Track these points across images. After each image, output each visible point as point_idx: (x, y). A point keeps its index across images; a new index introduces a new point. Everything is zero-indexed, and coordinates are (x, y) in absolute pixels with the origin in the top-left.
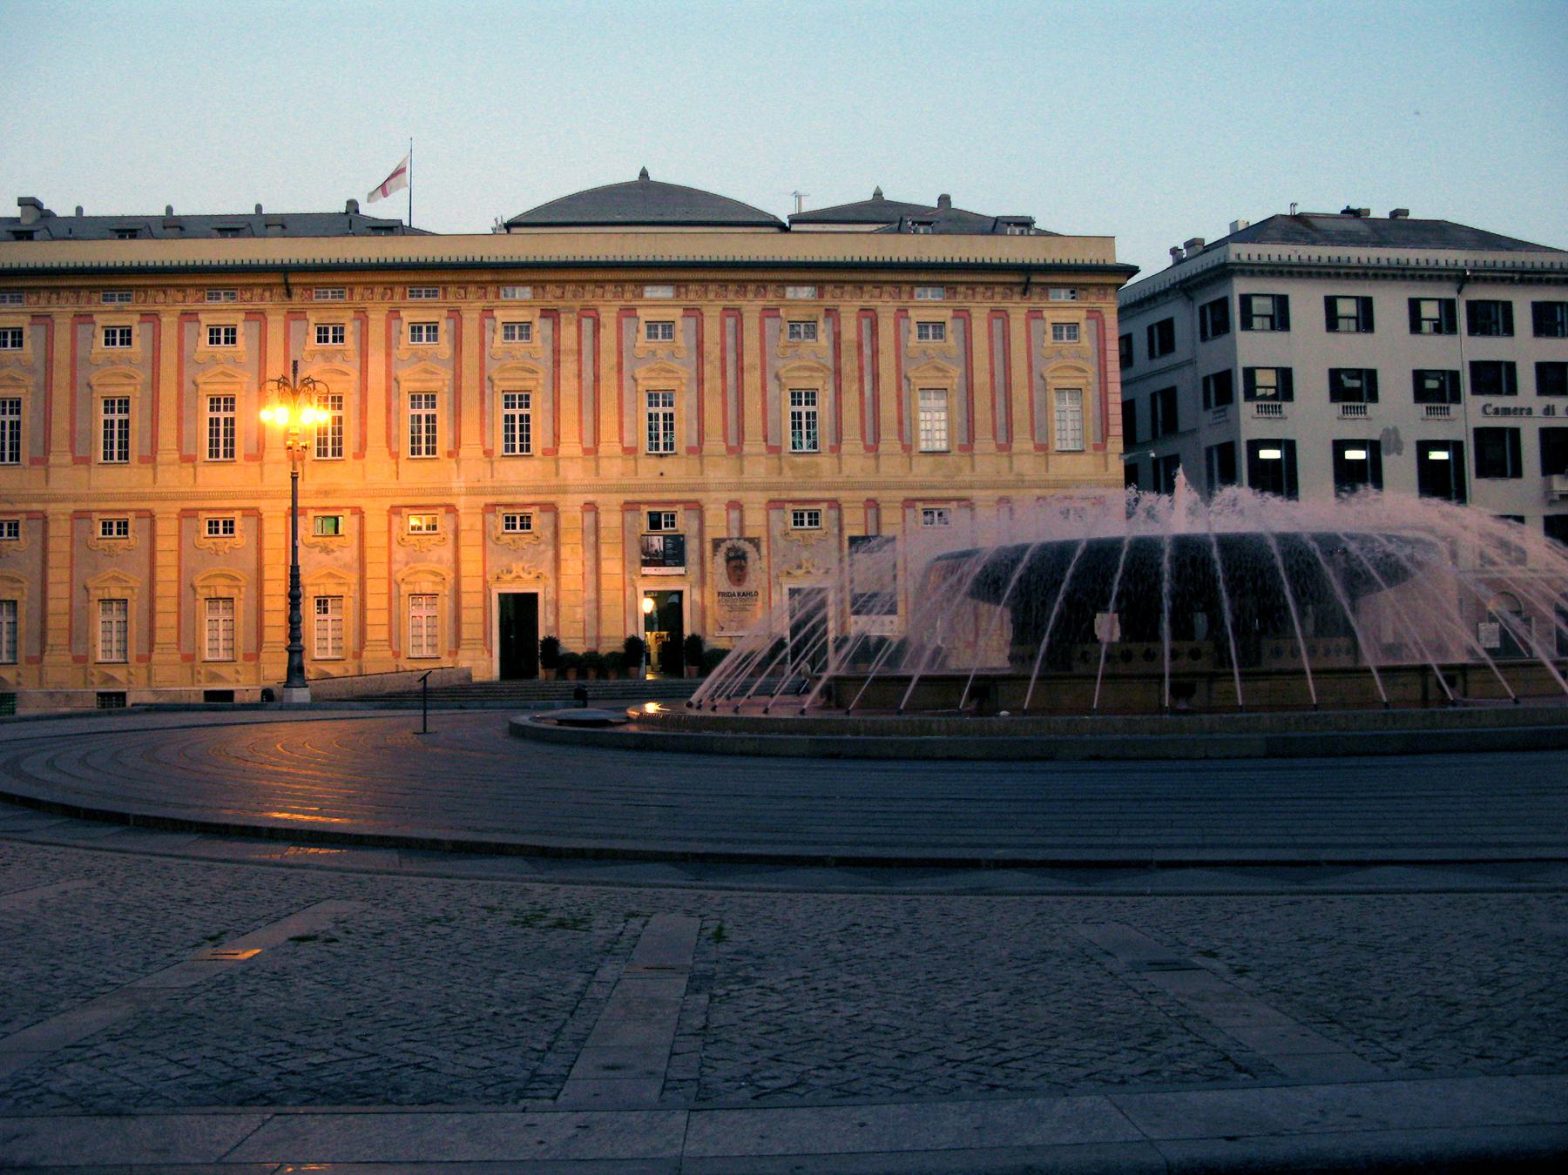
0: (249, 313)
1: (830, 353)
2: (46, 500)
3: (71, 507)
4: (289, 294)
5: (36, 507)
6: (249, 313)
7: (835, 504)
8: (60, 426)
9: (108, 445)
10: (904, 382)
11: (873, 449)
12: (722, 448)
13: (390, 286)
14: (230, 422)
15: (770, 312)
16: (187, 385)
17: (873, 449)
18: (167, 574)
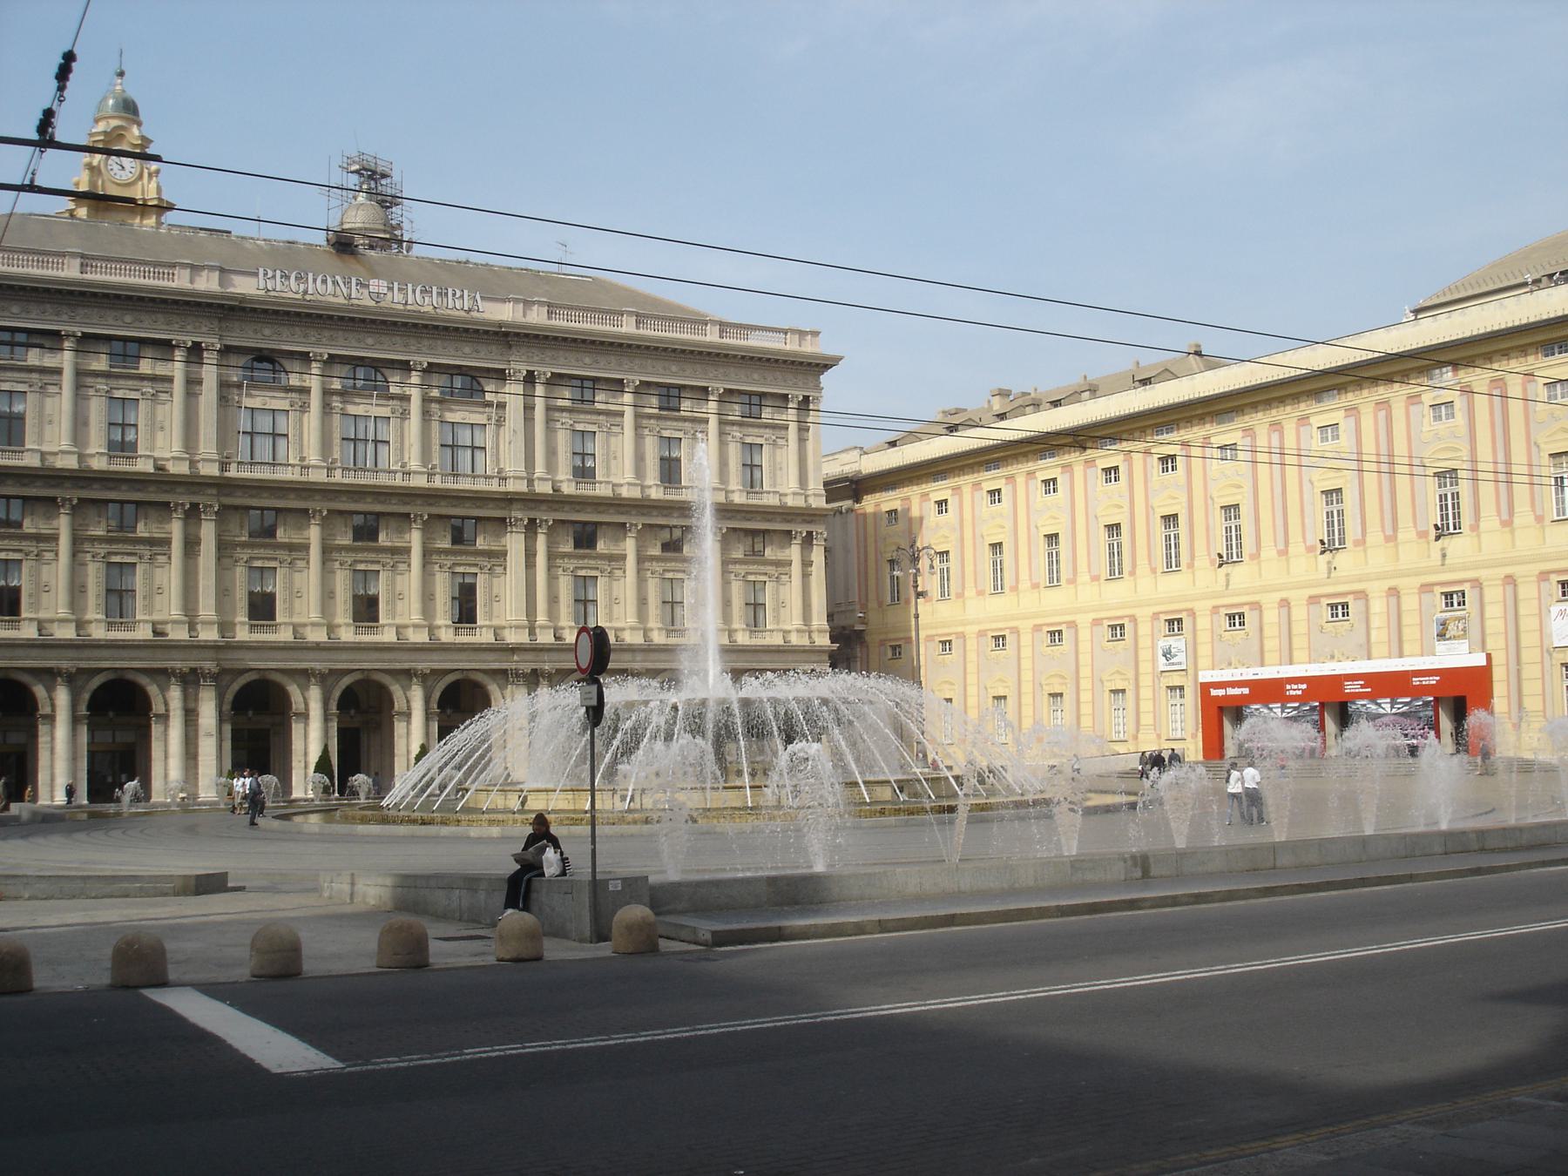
0: (1063, 466)
1: (1463, 431)
2: (963, 624)
3: (976, 628)
4: (1085, 449)
5: (960, 629)
6: (1063, 466)
7: (1477, 583)
8: (969, 569)
9: (995, 579)
10: (1534, 449)
11: (1508, 523)
12: (1381, 537)
13: (1143, 430)
14: (1341, 513)
15: (1414, 399)
16: (1033, 529)
17: (1508, 523)
18: (1027, 676)
